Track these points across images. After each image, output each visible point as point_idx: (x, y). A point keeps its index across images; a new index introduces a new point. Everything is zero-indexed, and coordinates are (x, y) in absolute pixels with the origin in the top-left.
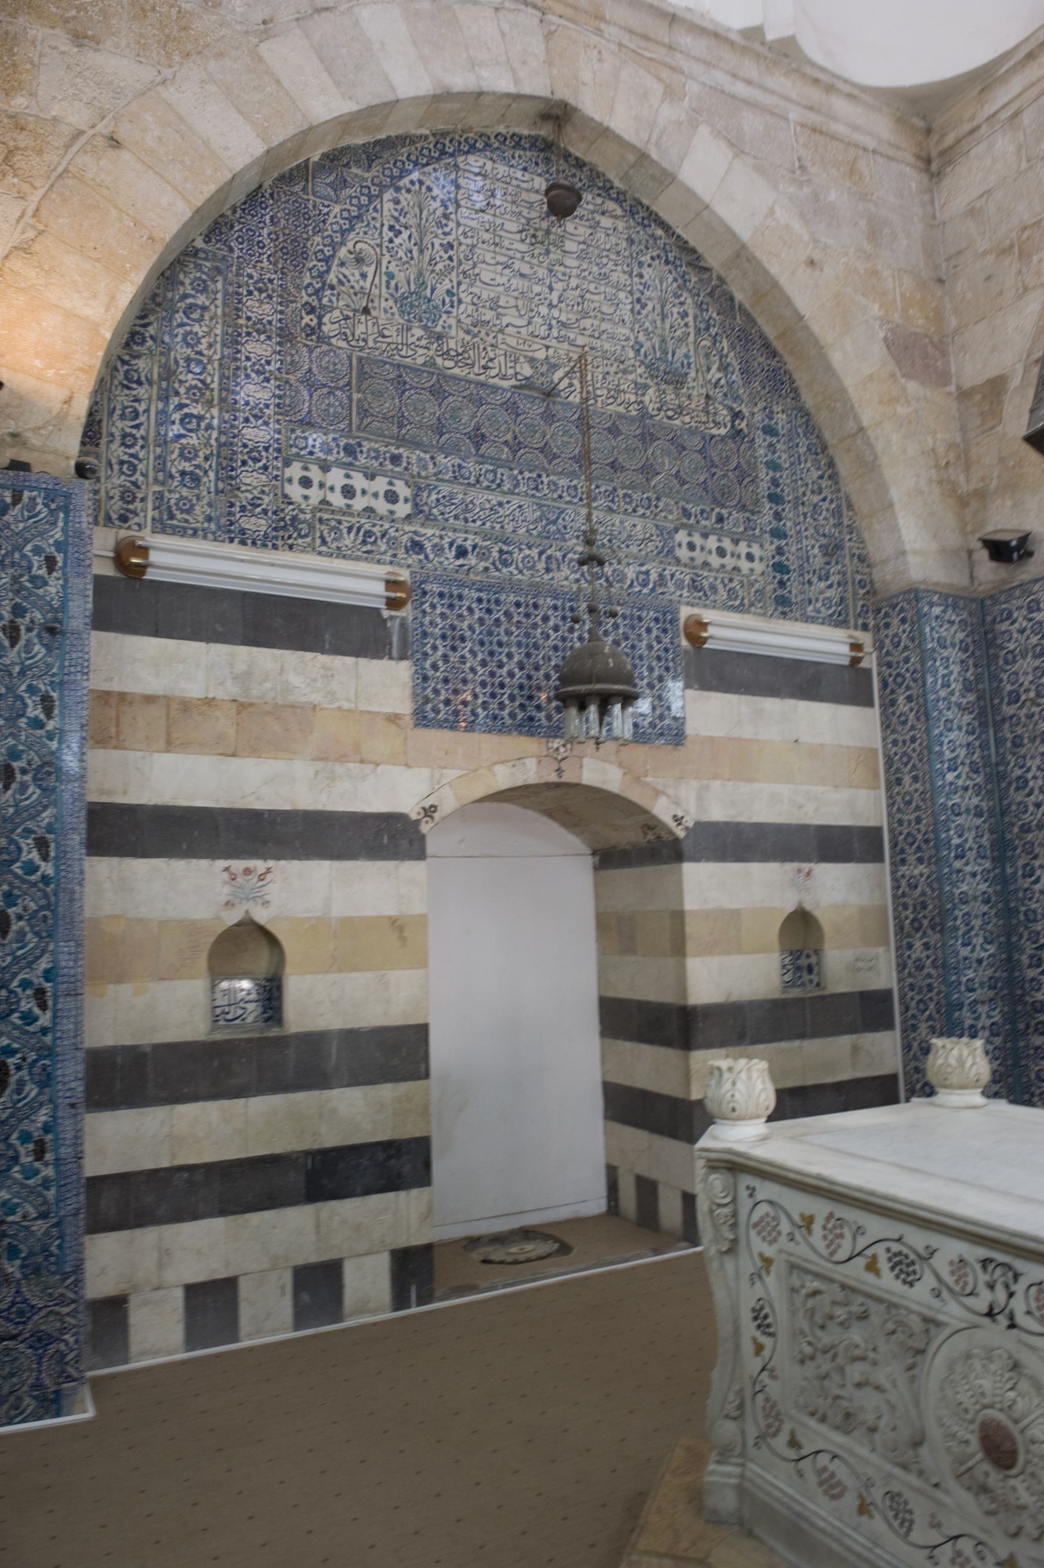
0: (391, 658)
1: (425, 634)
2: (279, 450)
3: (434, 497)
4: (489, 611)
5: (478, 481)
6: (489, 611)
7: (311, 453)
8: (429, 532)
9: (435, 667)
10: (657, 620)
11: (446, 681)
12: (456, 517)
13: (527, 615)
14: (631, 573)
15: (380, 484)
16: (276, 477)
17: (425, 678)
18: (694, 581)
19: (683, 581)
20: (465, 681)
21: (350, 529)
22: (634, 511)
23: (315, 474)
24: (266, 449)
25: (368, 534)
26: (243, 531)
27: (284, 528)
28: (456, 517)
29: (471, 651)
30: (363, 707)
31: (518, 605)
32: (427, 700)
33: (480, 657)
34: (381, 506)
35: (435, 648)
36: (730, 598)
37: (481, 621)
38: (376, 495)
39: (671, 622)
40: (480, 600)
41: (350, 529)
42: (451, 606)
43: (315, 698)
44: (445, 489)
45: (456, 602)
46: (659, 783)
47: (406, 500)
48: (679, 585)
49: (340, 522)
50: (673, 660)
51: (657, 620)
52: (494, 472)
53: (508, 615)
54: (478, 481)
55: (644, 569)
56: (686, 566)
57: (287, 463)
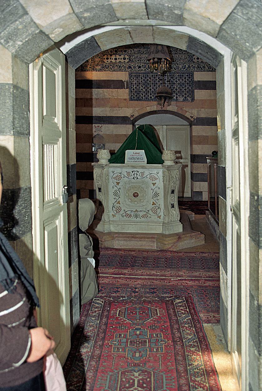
0: (124, 88)
1: (131, 84)
2: (102, 54)
3: (133, 57)
4: (146, 78)
5: (143, 53)
6: (146, 78)
7: (108, 53)
8: (133, 64)
9: (134, 90)
10: (187, 76)
11: (136, 92)
12: (138, 61)
13: (155, 78)
14: (181, 66)
15: (122, 57)
16: (102, 59)
17: (132, 92)
18: (198, 66)
19: (195, 66)
20: (140, 92)
21: (116, 66)
22: (182, 53)
23: (109, 57)
24: (100, 54)
25: (120, 66)
26: (96, 69)
27: (104, 67)
28: (138, 61)
29: (141, 86)
30: (119, 98)
31: (152, 76)
32: (132, 96)
33: (144, 87)
34: (122, 61)
35: (133, 86)
36: (209, 69)
37: (144, 80)
38: (121, 59)
39: (191, 76)
40: (144, 76)
41: (116, 66)
42: (137, 78)
43: (110, 97)
44: (136, 55)
45: (138, 77)
46: (187, 110)
47: (127, 59)
48: (194, 67)
49: (114, 65)
50: (192, 84)
51: (187, 76)
52: (147, 50)
53: (150, 78)
54: (143, 53)
55: (184, 65)
56: (196, 63)
57: (104, 56)
